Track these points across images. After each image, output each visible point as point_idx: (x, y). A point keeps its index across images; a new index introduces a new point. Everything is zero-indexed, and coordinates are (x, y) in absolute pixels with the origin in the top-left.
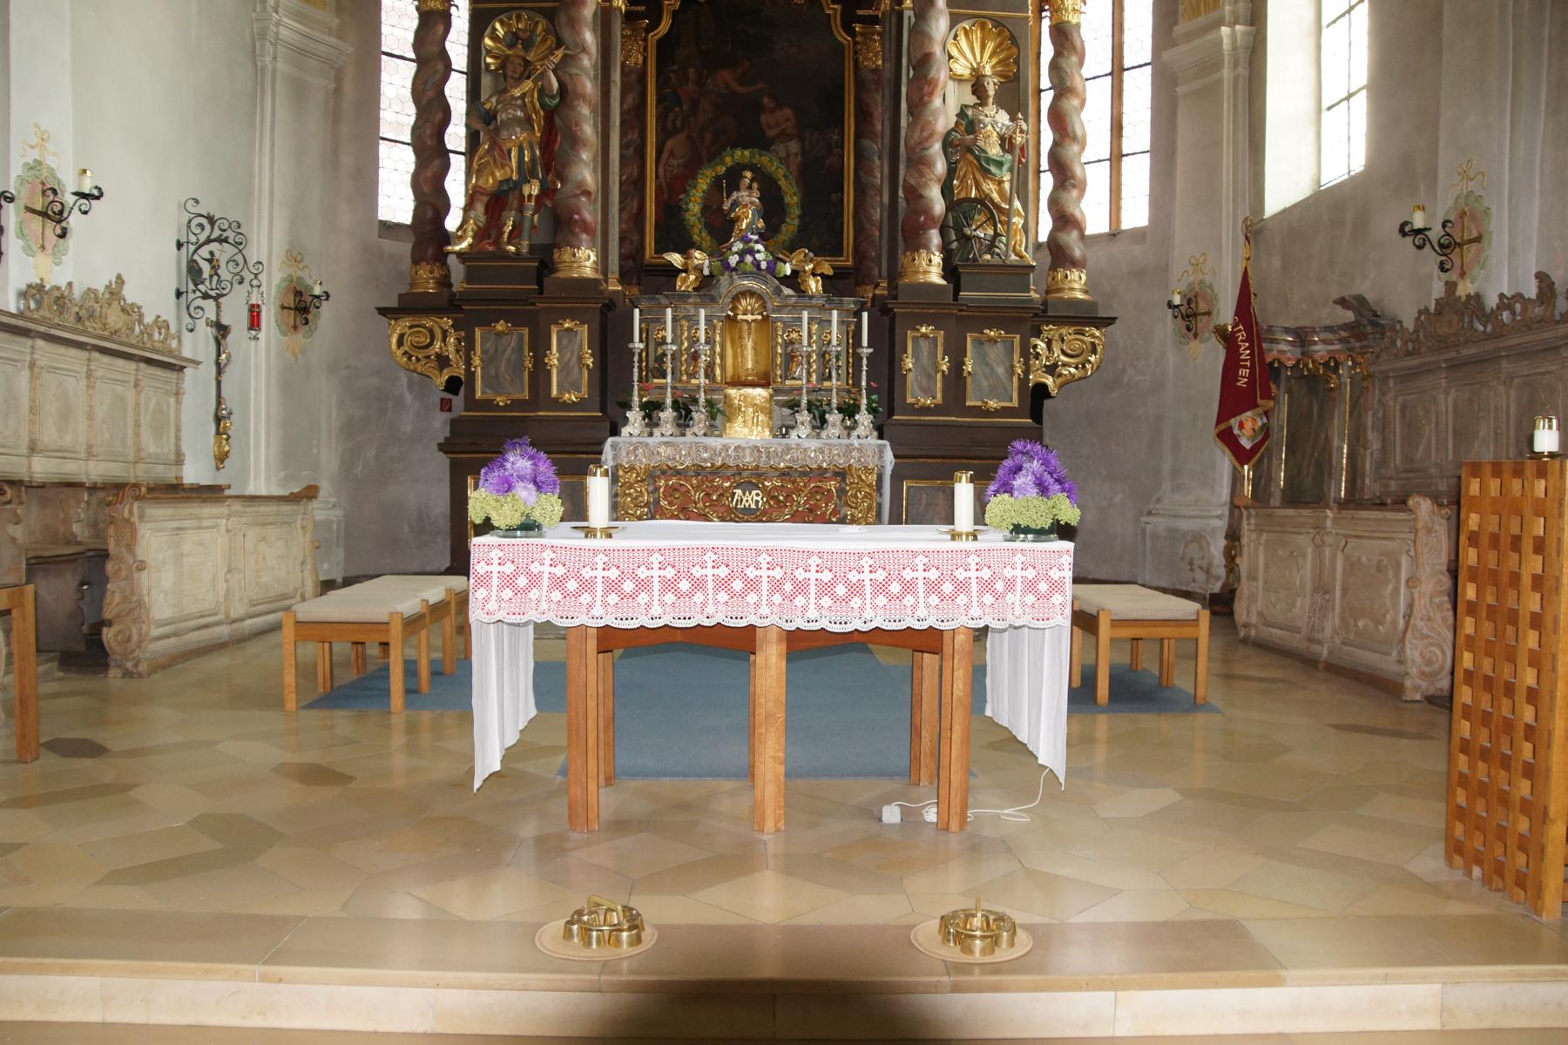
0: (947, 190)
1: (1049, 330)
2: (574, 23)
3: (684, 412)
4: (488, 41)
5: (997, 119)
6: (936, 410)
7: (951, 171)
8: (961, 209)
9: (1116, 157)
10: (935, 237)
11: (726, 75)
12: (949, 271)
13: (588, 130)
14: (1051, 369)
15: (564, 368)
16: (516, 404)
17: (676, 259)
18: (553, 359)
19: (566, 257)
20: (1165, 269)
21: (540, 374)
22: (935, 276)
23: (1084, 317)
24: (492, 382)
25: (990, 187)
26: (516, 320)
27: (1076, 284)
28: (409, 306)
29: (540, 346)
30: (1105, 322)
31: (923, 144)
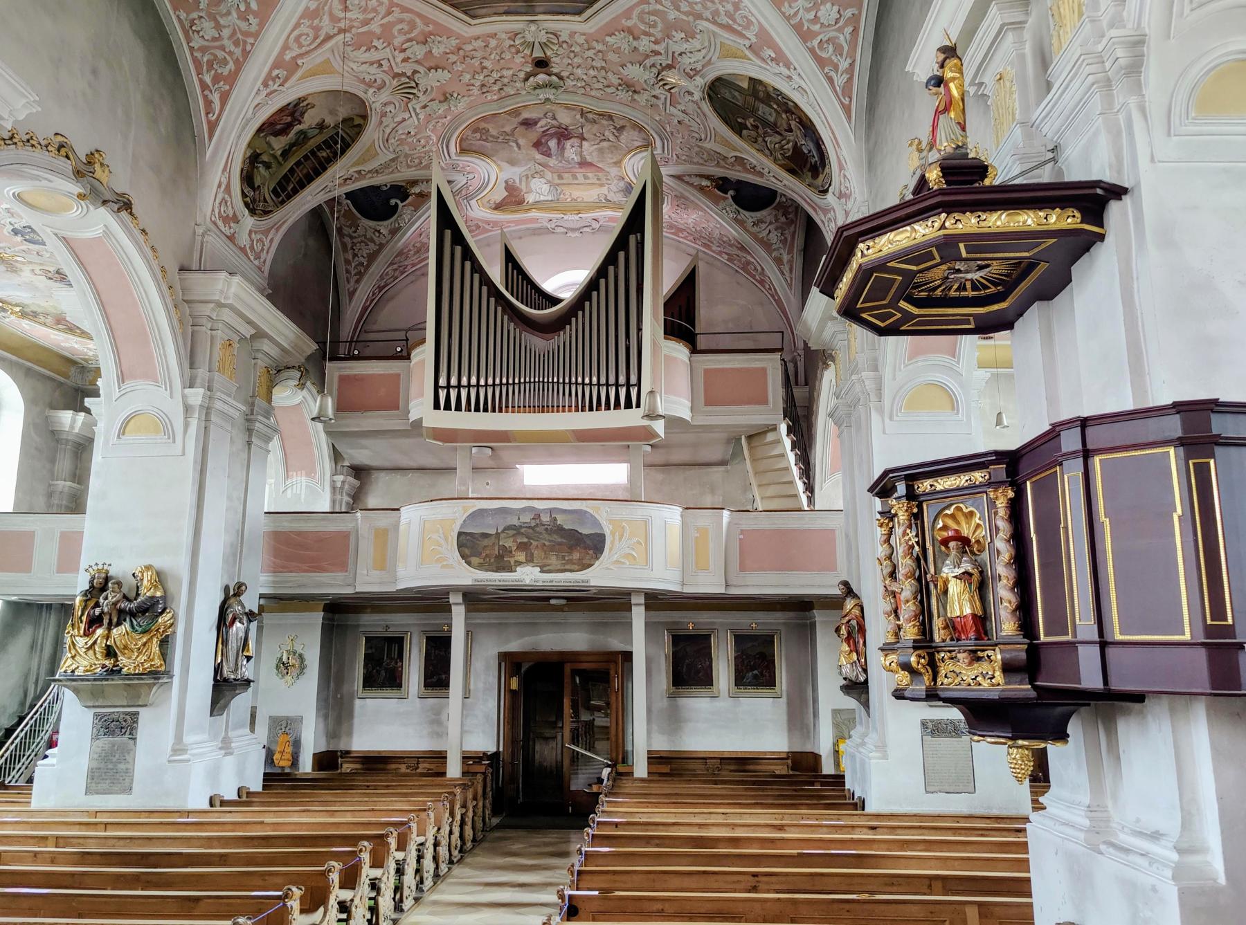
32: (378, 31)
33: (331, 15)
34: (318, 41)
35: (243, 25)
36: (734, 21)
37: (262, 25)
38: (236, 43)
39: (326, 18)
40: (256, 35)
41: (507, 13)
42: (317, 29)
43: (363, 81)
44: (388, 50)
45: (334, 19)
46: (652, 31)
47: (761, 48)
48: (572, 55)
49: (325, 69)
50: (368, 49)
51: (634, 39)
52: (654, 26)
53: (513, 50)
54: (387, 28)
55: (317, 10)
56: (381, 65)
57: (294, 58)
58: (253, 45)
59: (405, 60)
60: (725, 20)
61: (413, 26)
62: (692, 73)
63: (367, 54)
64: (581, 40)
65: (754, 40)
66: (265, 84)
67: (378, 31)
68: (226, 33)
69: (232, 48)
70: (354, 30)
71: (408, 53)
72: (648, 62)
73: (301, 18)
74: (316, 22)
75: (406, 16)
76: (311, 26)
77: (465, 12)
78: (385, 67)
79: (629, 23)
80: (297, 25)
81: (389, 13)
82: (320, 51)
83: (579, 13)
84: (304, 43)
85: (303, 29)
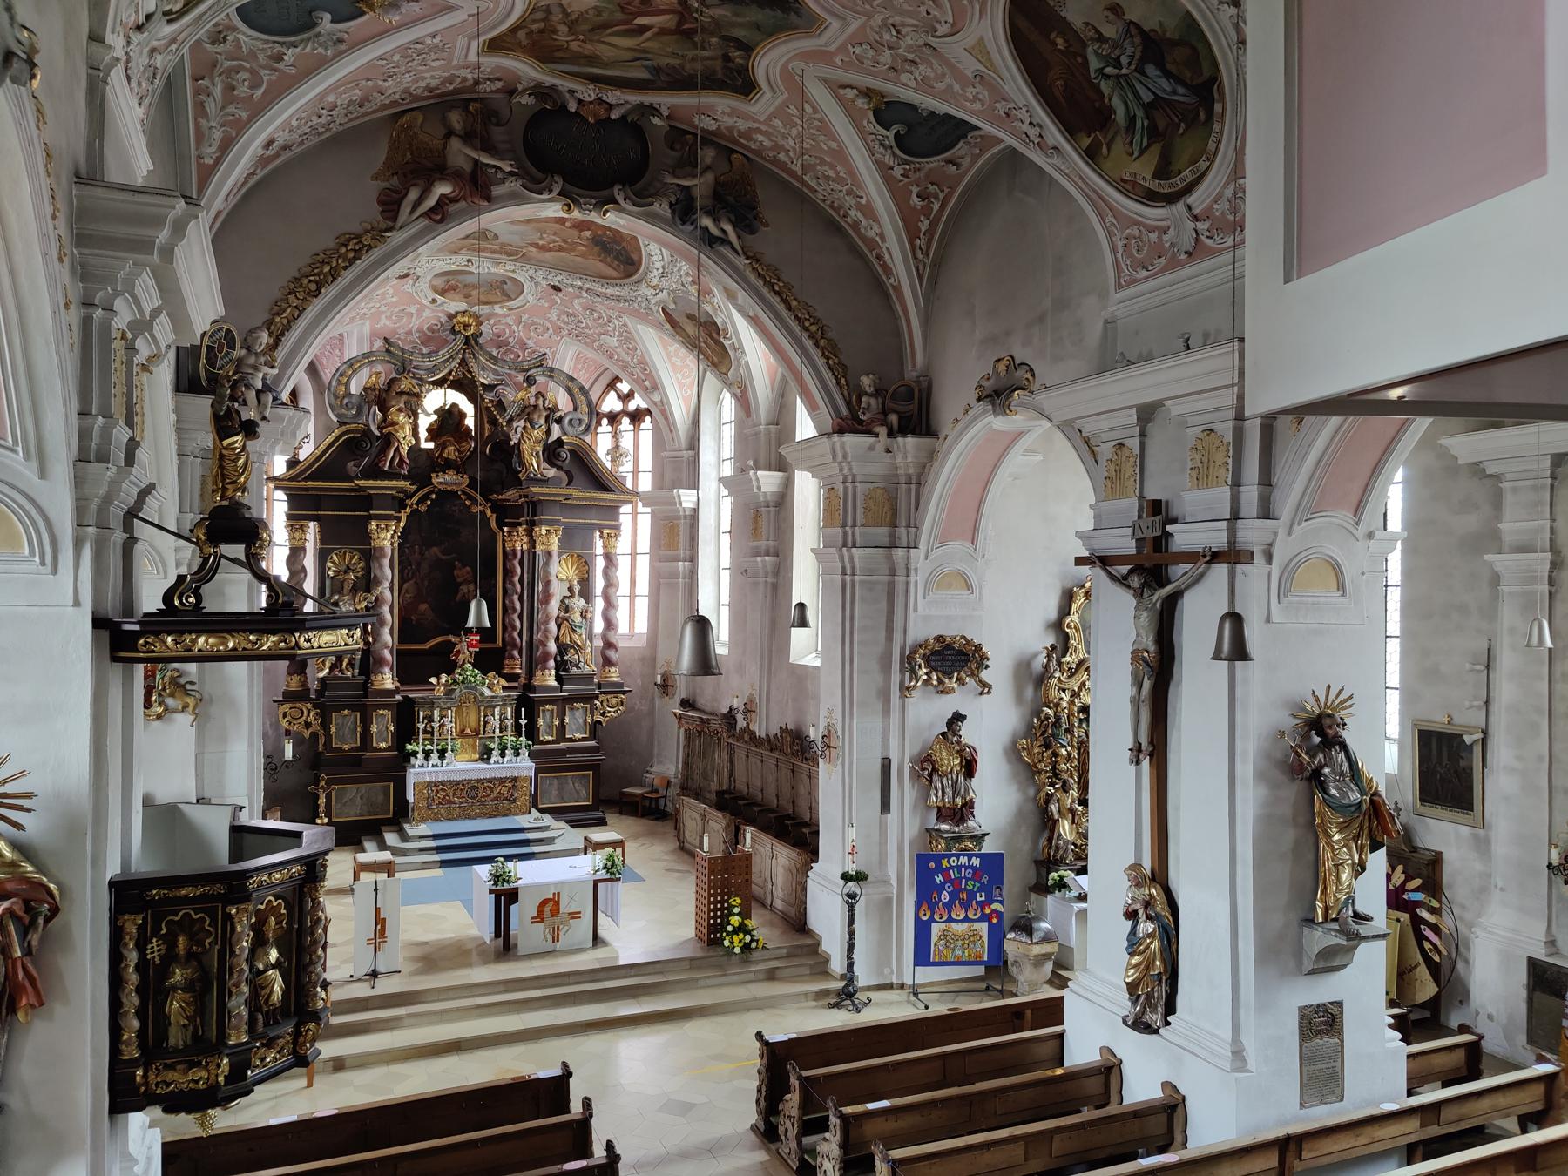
0: (557, 639)
1: (602, 697)
2: (381, 567)
3: (442, 753)
4: (329, 564)
5: (578, 603)
6: (553, 742)
7: (559, 627)
8: (563, 648)
9: (633, 597)
10: (552, 663)
11: (435, 549)
12: (559, 679)
13: (388, 617)
14: (603, 714)
15: (379, 732)
16: (352, 749)
17: (433, 680)
18: (374, 728)
19: (379, 677)
20: (654, 659)
21: (366, 735)
22: (552, 682)
23: (617, 689)
24: (342, 739)
25: (576, 637)
26: (352, 708)
27: (614, 675)
28: (289, 697)
29: (366, 723)
30: (624, 693)
31: (547, 622)
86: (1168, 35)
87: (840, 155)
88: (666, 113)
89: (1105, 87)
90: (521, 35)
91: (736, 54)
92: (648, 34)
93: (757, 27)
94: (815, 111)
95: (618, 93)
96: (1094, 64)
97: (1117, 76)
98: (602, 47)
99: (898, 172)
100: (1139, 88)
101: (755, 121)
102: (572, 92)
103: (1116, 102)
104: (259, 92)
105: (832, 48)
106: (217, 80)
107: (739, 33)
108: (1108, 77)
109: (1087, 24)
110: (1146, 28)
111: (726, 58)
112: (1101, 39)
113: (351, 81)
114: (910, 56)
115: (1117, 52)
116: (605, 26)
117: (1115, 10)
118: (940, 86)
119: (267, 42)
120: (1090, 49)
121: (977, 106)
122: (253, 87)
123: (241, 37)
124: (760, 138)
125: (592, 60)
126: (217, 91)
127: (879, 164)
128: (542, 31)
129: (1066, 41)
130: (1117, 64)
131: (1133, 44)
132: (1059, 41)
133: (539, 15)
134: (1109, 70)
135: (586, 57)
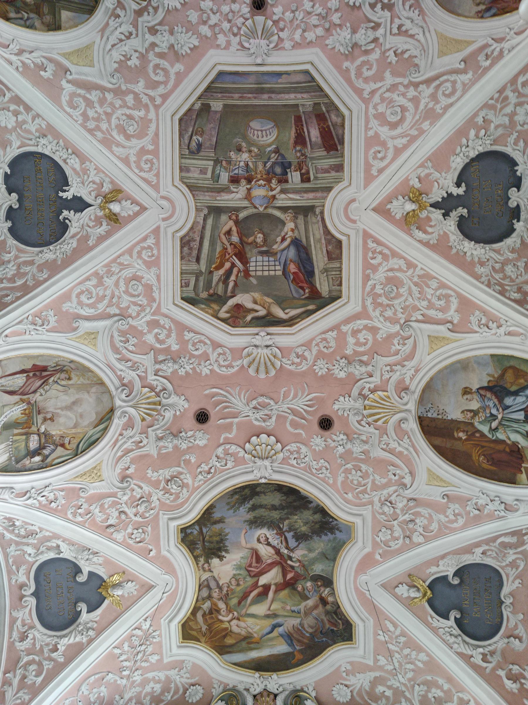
32: (387, 74)
33: (417, 108)
34: (437, 82)
35: (491, 116)
36: (85, 99)
37: (476, 115)
38: (506, 98)
39: (422, 107)
40: (486, 106)
41: (279, 74)
42: (434, 97)
43: (422, 13)
44: (388, 47)
45: (415, 101)
46: (158, 61)
47: (55, 74)
48: (230, 16)
49: (448, 45)
50: (403, 52)
51: (172, 46)
52: (157, 66)
53: (281, 24)
54: (379, 77)
55: (425, 119)
56: (400, 27)
57: (465, 71)
58: (492, 99)
59: (377, 26)
60: (94, 96)
61: (359, 74)
62: (119, 11)
63: (406, 47)
64: (221, 39)
65: (64, 83)
66: (501, 55)
67: (387, 74)
68: (508, 110)
69: (511, 95)
70: (406, 82)
71: (371, 35)
72: (161, 14)
73: (442, 115)
74: (431, 105)
75: (360, 84)
76: (437, 102)
77: (313, 79)
78: (397, 22)
79: (179, 67)
80: (446, 108)
81: (373, 92)
82: (442, 70)
83: (221, 74)
84: (448, 85)
85: (444, 101)
86: (496, 376)
87: (432, 665)
88: (313, 694)
89: (501, 435)
90: (199, 615)
91: (326, 592)
92: (271, 594)
93: (324, 556)
94: (395, 626)
95: (275, 676)
96: (485, 429)
97: (500, 423)
98: (250, 621)
99: (478, 660)
100: (514, 416)
101: (368, 669)
102: (247, 690)
103: (515, 437)
104: (40, 679)
105: (368, 549)
106: (18, 672)
107: (318, 569)
108: (497, 428)
109: (463, 412)
110: (486, 385)
111: (323, 601)
112: (475, 413)
113: (99, 672)
114: (407, 517)
115: (488, 411)
116: (245, 596)
117: (466, 391)
118: (434, 526)
119: (50, 636)
120: (476, 424)
121: (461, 522)
122: (37, 676)
123: (36, 633)
124: (380, 689)
125: (248, 641)
126: (16, 682)
127: (461, 655)
128: (211, 613)
129: (463, 431)
130: (494, 417)
131: (489, 399)
132: (461, 434)
133: (205, 593)
134: (494, 424)
135: (245, 638)
